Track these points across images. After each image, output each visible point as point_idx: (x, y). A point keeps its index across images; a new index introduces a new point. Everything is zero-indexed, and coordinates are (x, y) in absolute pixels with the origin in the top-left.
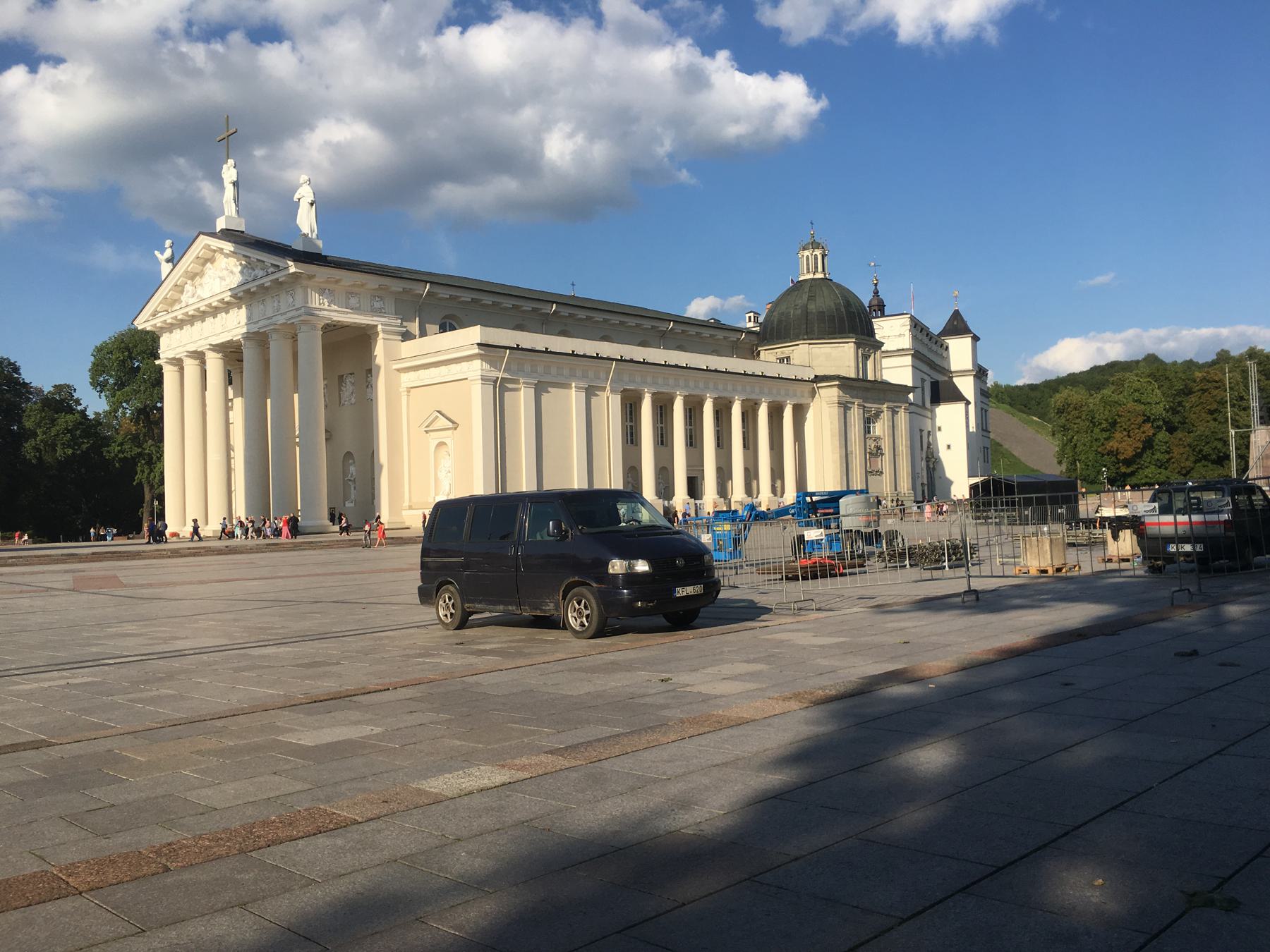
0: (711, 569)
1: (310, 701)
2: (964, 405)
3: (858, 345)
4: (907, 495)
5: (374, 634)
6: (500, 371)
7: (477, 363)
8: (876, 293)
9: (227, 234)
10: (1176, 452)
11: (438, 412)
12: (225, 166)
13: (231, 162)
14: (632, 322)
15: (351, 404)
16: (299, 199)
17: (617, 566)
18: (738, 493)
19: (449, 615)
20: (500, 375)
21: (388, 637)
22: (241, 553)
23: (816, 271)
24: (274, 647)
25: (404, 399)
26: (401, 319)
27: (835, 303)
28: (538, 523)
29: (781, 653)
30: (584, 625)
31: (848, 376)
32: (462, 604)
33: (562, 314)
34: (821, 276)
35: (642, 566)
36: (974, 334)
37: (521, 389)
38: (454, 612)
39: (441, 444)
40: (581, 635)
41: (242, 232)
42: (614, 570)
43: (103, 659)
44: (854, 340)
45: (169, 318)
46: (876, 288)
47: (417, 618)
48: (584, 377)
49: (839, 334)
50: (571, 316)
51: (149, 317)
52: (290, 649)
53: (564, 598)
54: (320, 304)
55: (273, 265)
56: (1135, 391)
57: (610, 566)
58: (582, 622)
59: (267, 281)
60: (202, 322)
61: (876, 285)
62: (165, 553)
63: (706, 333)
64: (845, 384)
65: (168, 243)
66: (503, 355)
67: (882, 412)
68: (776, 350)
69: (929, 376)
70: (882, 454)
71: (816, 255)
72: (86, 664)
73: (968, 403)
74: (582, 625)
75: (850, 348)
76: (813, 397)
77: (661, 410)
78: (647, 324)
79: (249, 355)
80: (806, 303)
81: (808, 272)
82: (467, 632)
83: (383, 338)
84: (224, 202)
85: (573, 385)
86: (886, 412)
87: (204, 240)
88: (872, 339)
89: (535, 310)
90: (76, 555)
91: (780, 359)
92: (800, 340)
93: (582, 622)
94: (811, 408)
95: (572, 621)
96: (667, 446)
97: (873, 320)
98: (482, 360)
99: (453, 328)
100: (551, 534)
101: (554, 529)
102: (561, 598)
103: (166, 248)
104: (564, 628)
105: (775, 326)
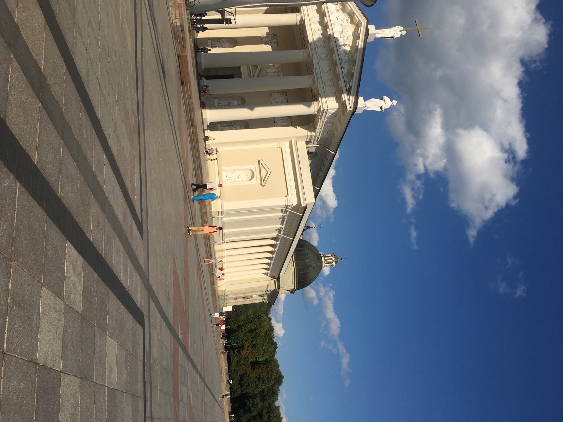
6: (290, 210)
10: (244, 367)
12: (402, 28)
16: (384, 101)
20: (289, 210)
23: (325, 263)
25: (275, 145)
44: (295, 289)
46: (311, 227)
55: (350, 88)
56: (268, 349)
59: (342, 83)
61: (312, 227)
66: (299, 211)
76: (270, 277)
83: (308, 136)
84: (384, 30)
85: (282, 226)
92: (296, 267)
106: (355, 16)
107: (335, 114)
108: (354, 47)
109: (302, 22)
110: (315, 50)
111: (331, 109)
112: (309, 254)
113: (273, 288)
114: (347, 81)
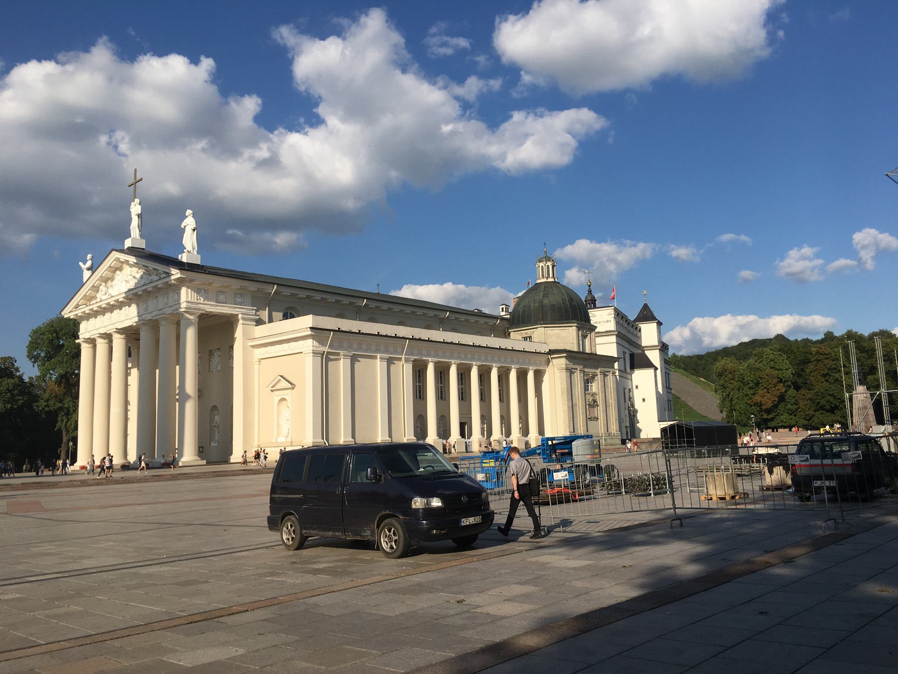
0: (487, 504)
1: (187, 622)
2: (653, 370)
3: (579, 328)
4: (616, 435)
5: (234, 554)
7: (310, 342)
8: (590, 291)
9: (132, 251)
10: (802, 403)
11: (281, 376)
12: (132, 203)
13: (137, 201)
14: (420, 312)
15: (218, 371)
16: (185, 227)
17: (418, 503)
18: (497, 433)
19: (290, 539)
20: (326, 349)
21: (243, 557)
22: (133, 482)
24: (158, 566)
25: (256, 366)
27: (562, 299)
28: (360, 466)
29: (545, 575)
30: (394, 548)
31: (572, 350)
32: (301, 530)
33: (371, 306)
34: (552, 280)
35: (436, 503)
36: (659, 321)
37: (341, 359)
38: (294, 536)
39: (283, 399)
40: (391, 555)
41: (143, 249)
42: (416, 505)
43: (27, 577)
44: (576, 325)
45: (87, 310)
46: (590, 288)
47: (266, 539)
48: (386, 351)
49: (565, 320)
50: (377, 307)
52: (170, 568)
53: (378, 527)
54: (197, 300)
56: (771, 360)
57: (413, 503)
58: (391, 545)
59: (160, 284)
60: (111, 313)
61: (589, 286)
62: (76, 483)
63: (473, 319)
64: (571, 356)
65: (89, 256)
67: (597, 375)
68: (522, 332)
69: (628, 349)
70: (598, 405)
71: (548, 265)
72: (13, 581)
73: (656, 369)
74: (392, 547)
75: (573, 330)
76: (548, 365)
77: (441, 374)
78: (431, 313)
79: (144, 335)
80: (542, 298)
81: (543, 277)
82: (305, 552)
83: (243, 324)
84: (131, 228)
85: (378, 357)
86: (599, 375)
87: (115, 255)
88: (588, 324)
89: (351, 303)
90: (7, 485)
91: (524, 338)
92: (538, 325)
93: (391, 545)
94: (547, 372)
95: (384, 545)
96: (445, 400)
97: (589, 311)
98: (313, 339)
99: (292, 317)
100: (369, 478)
101: (371, 474)
102: (376, 527)
103: (88, 260)
104: (378, 549)
105: (521, 315)
106: (112, 265)
107: (198, 291)
108: (136, 265)
109: (120, 331)
112: (524, 304)
113: (563, 361)
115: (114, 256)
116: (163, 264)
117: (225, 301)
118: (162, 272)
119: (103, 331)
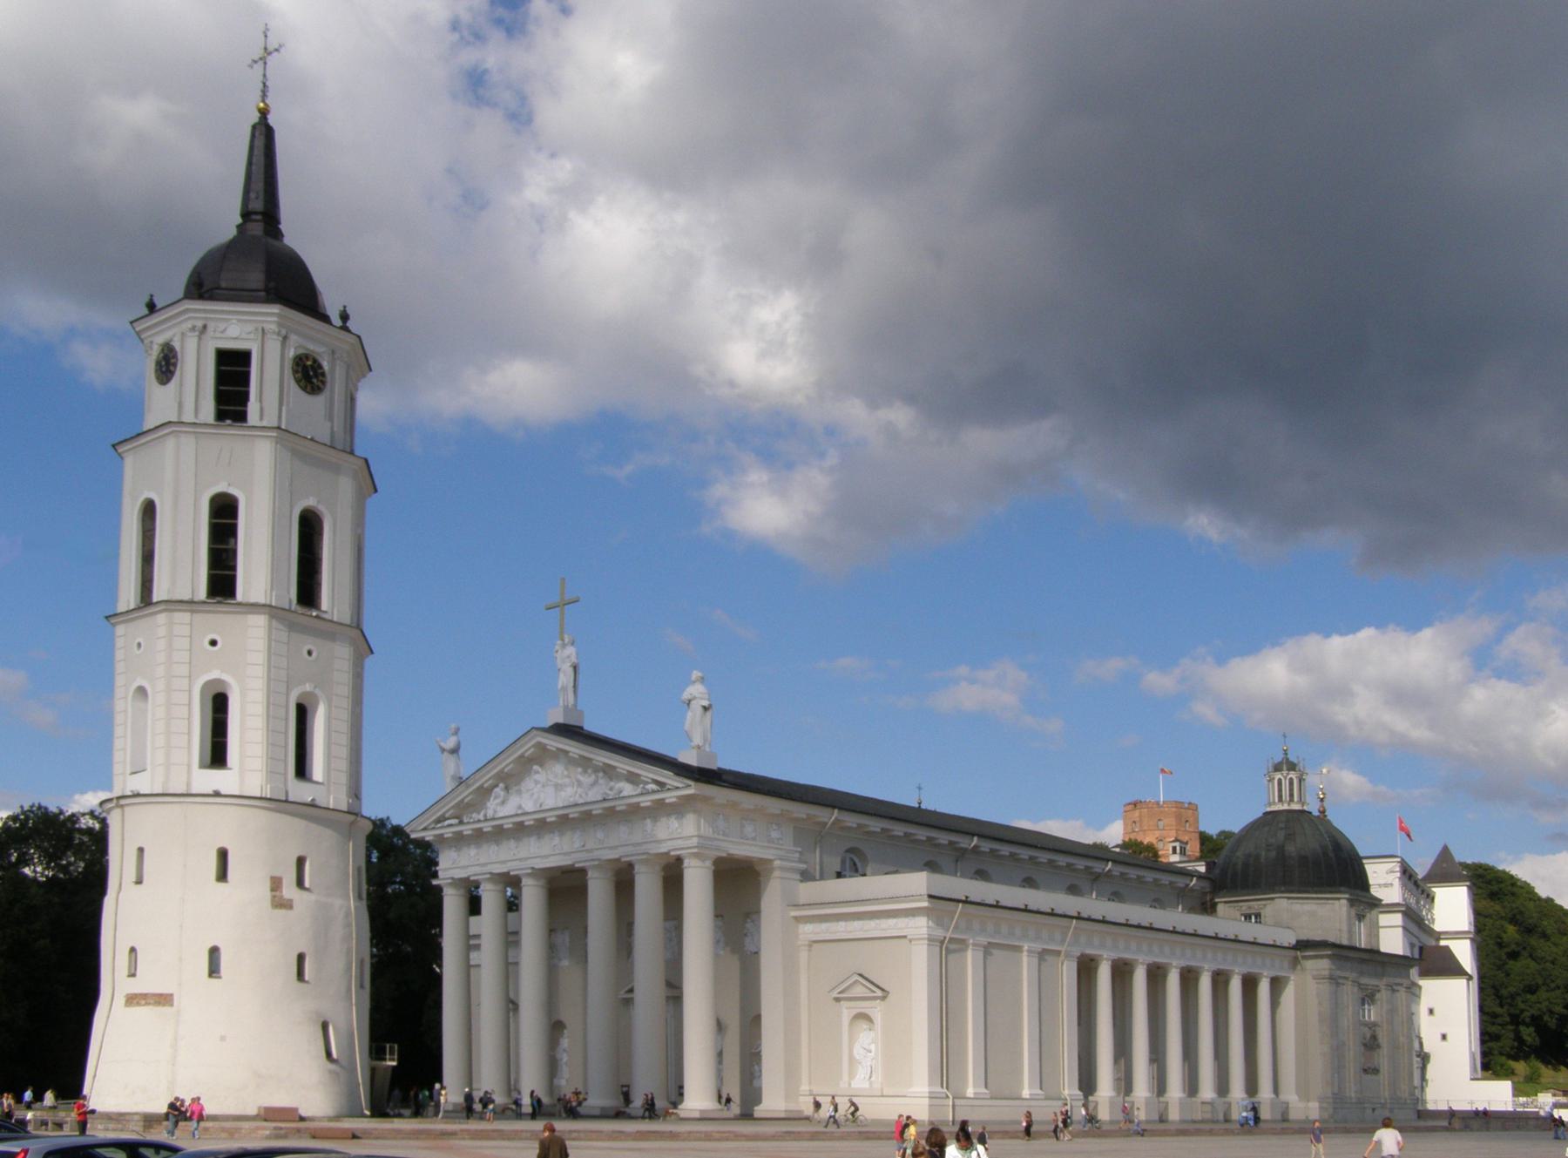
20: (948, 935)
26: (800, 852)
45: (467, 830)
51: (430, 824)
83: (782, 878)
85: (1026, 948)
98: (928, 916)
106: (526, 755)
109: (537, 873)
110: (587, 851)
111: (699, 829)
114: (643, 788)
115: (533, 738)
116: (624, 756)
117: (753, 835)
118: (650, 781)
119: (499, 869)
